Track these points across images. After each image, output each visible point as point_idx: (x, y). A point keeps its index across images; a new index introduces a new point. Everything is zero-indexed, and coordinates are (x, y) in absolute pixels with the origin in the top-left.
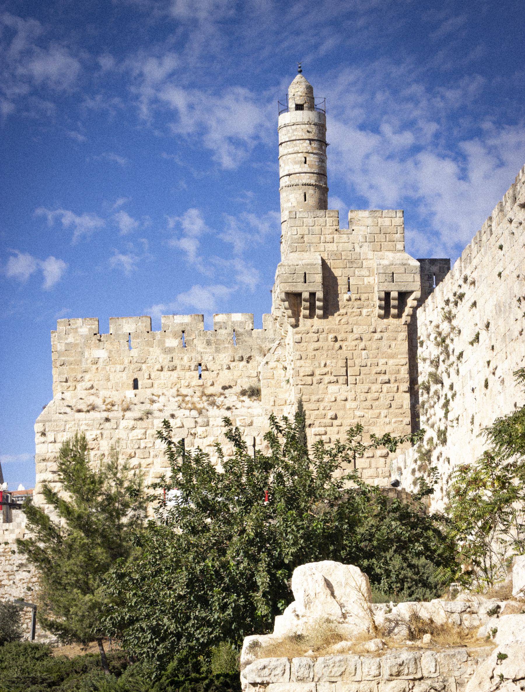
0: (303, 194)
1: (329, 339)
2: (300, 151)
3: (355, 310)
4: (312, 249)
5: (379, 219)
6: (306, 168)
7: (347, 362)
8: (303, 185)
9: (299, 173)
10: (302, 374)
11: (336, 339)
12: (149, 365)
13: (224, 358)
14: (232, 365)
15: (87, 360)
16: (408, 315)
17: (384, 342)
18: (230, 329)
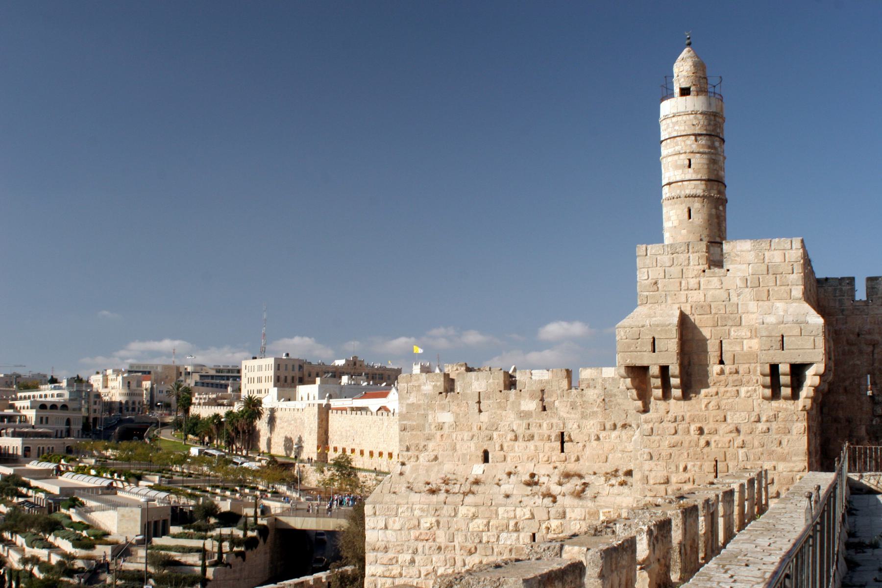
0: (686, 210)
1: (692, 432)
2: (681, 152)
3: (729, 388)
4: (669, 301)
5: (767, 253)
6: (690, 174)
7: (716, 466)
8: (686, 197)
9: (682, 181)
10: (651, 482)
11: (701, 431)
12: (501, 433)
13: (592, 426)
14: (602, 435)
15: (430, 425)
16: (806, 398)
17: (774, 435)
18: (600, 388)
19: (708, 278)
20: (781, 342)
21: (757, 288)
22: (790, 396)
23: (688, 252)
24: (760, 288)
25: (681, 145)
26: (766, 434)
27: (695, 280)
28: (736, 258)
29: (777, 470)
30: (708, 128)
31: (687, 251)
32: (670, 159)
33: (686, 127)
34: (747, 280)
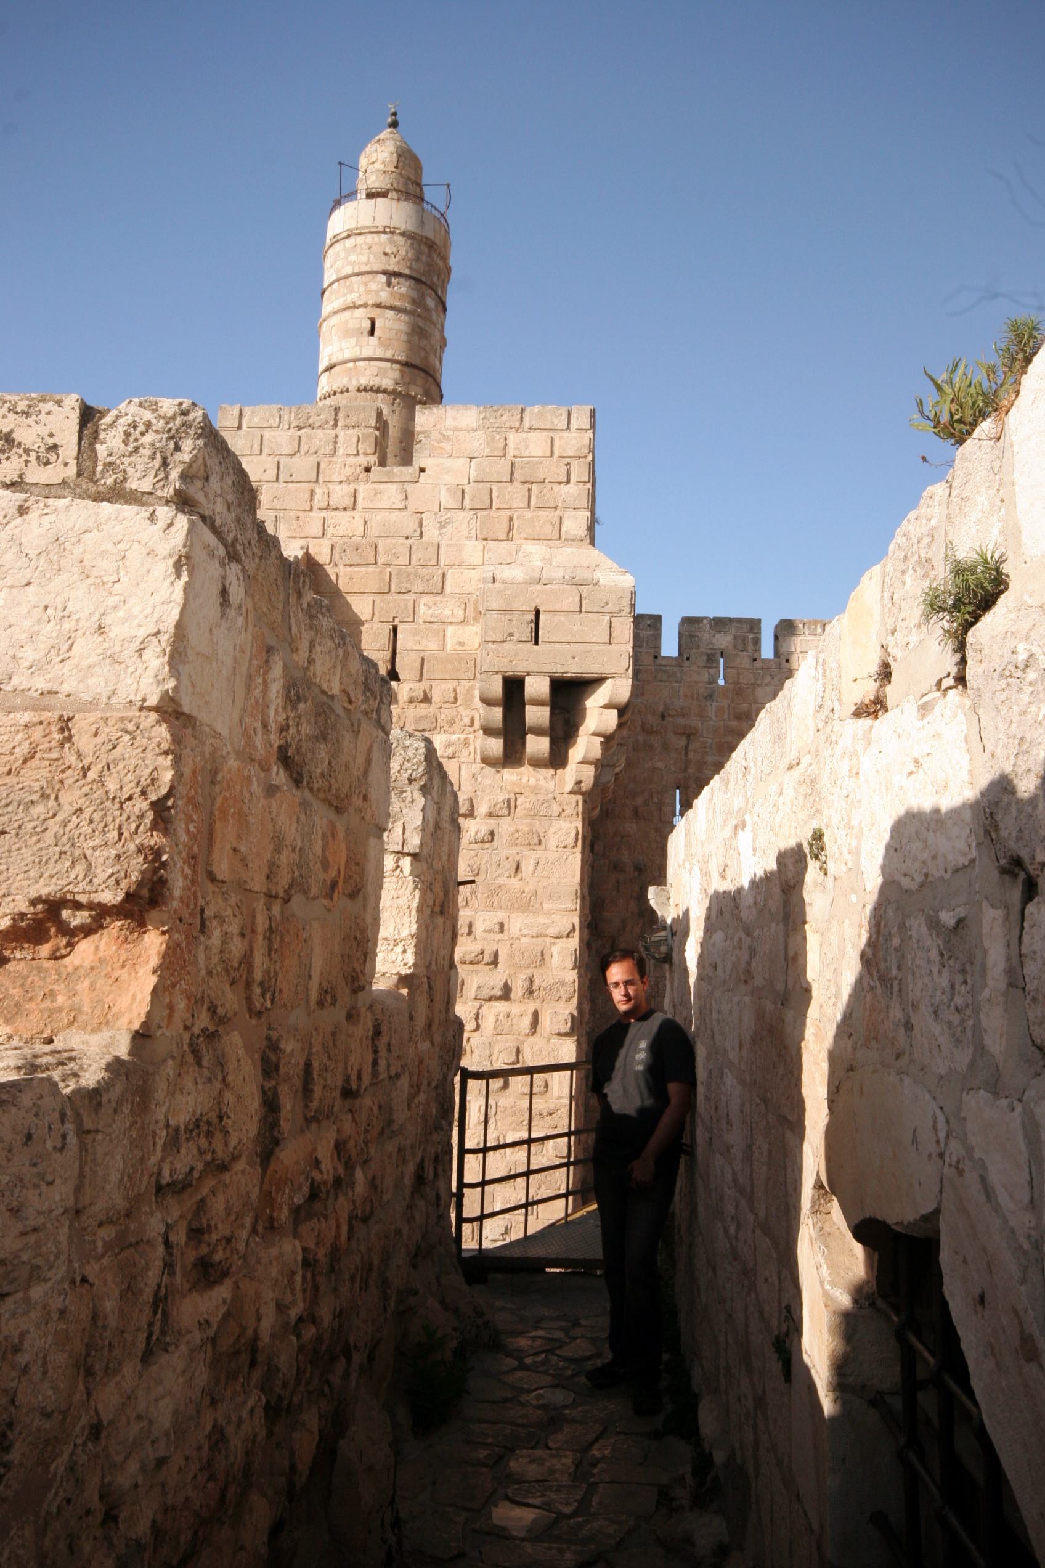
2: (358, 303)
5: (512, 436)
6: (371, 347)
8: (359, 390)
17: (503, 850)
19: (375, 486)
20: (533, 625)
21: (484, 513)
22: (547, 755)
23: (335, 425)
24: (493, 513)
25: (358, 292)
26: (486, 845)
27: (348, 489)
28: (442, 445)
29: (506, 932)
30: (414, 265)
31: (332, 423)
32: (334, 320)
33: (372, 257)
34: (463, 492)
